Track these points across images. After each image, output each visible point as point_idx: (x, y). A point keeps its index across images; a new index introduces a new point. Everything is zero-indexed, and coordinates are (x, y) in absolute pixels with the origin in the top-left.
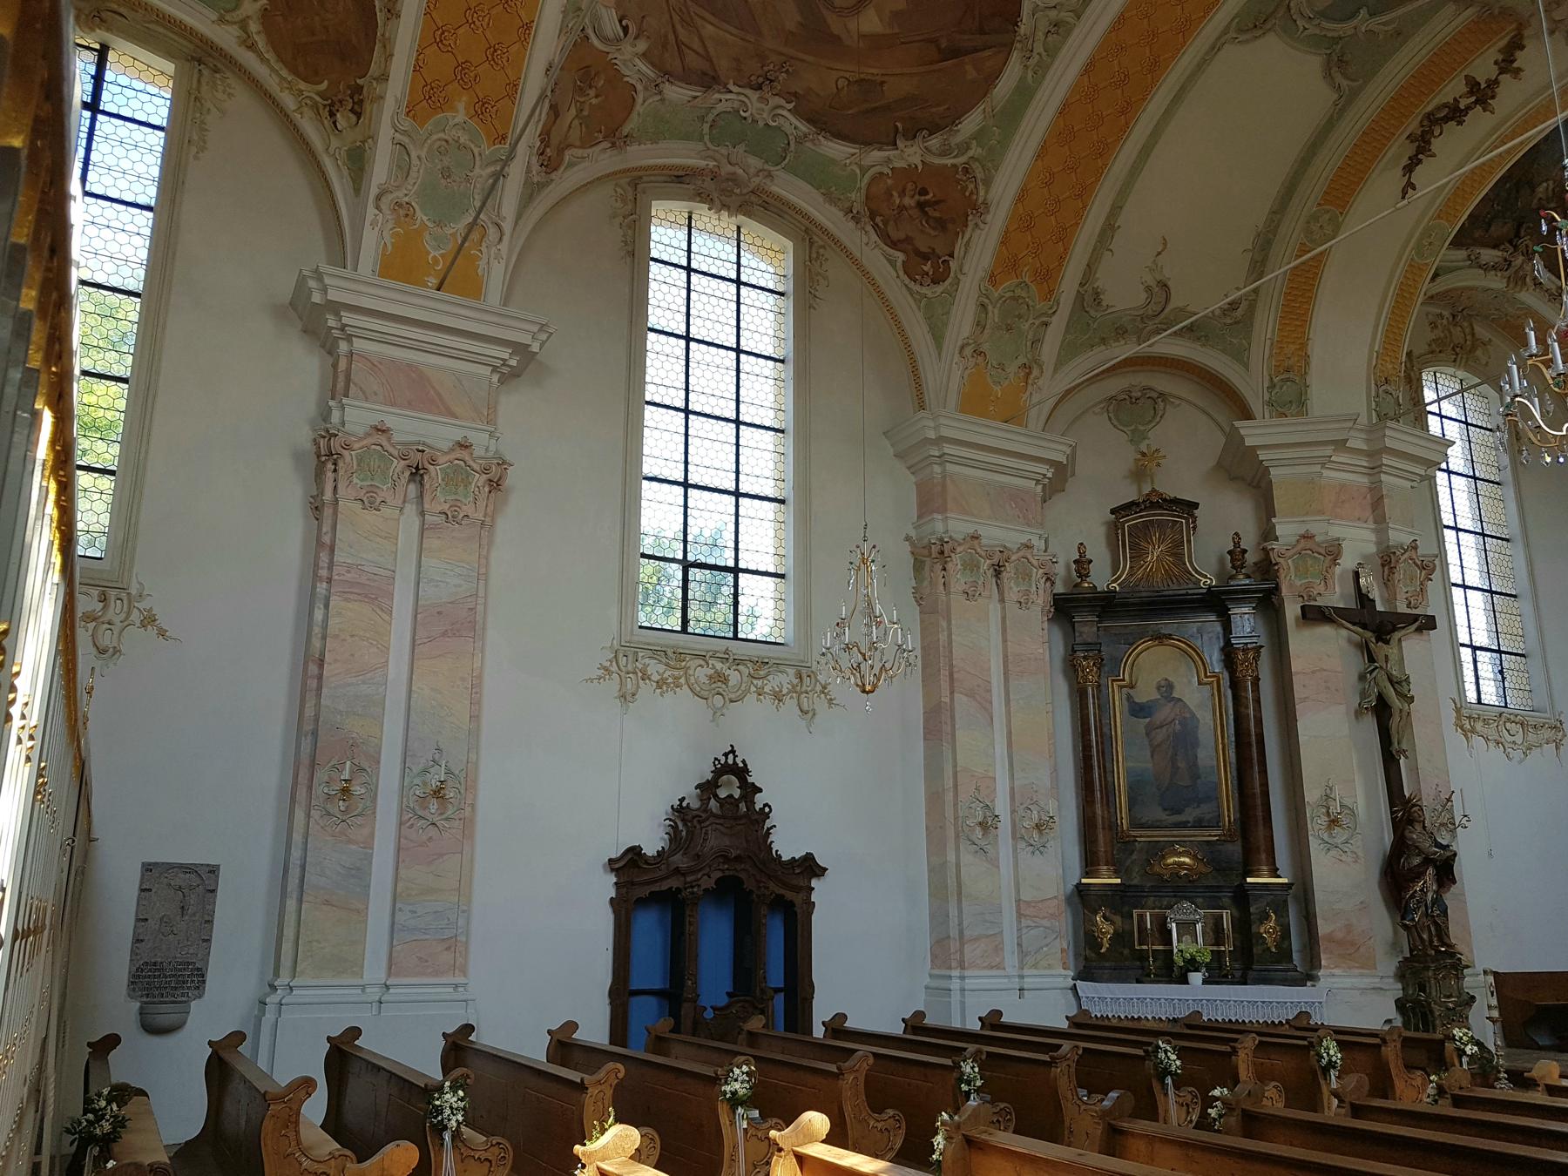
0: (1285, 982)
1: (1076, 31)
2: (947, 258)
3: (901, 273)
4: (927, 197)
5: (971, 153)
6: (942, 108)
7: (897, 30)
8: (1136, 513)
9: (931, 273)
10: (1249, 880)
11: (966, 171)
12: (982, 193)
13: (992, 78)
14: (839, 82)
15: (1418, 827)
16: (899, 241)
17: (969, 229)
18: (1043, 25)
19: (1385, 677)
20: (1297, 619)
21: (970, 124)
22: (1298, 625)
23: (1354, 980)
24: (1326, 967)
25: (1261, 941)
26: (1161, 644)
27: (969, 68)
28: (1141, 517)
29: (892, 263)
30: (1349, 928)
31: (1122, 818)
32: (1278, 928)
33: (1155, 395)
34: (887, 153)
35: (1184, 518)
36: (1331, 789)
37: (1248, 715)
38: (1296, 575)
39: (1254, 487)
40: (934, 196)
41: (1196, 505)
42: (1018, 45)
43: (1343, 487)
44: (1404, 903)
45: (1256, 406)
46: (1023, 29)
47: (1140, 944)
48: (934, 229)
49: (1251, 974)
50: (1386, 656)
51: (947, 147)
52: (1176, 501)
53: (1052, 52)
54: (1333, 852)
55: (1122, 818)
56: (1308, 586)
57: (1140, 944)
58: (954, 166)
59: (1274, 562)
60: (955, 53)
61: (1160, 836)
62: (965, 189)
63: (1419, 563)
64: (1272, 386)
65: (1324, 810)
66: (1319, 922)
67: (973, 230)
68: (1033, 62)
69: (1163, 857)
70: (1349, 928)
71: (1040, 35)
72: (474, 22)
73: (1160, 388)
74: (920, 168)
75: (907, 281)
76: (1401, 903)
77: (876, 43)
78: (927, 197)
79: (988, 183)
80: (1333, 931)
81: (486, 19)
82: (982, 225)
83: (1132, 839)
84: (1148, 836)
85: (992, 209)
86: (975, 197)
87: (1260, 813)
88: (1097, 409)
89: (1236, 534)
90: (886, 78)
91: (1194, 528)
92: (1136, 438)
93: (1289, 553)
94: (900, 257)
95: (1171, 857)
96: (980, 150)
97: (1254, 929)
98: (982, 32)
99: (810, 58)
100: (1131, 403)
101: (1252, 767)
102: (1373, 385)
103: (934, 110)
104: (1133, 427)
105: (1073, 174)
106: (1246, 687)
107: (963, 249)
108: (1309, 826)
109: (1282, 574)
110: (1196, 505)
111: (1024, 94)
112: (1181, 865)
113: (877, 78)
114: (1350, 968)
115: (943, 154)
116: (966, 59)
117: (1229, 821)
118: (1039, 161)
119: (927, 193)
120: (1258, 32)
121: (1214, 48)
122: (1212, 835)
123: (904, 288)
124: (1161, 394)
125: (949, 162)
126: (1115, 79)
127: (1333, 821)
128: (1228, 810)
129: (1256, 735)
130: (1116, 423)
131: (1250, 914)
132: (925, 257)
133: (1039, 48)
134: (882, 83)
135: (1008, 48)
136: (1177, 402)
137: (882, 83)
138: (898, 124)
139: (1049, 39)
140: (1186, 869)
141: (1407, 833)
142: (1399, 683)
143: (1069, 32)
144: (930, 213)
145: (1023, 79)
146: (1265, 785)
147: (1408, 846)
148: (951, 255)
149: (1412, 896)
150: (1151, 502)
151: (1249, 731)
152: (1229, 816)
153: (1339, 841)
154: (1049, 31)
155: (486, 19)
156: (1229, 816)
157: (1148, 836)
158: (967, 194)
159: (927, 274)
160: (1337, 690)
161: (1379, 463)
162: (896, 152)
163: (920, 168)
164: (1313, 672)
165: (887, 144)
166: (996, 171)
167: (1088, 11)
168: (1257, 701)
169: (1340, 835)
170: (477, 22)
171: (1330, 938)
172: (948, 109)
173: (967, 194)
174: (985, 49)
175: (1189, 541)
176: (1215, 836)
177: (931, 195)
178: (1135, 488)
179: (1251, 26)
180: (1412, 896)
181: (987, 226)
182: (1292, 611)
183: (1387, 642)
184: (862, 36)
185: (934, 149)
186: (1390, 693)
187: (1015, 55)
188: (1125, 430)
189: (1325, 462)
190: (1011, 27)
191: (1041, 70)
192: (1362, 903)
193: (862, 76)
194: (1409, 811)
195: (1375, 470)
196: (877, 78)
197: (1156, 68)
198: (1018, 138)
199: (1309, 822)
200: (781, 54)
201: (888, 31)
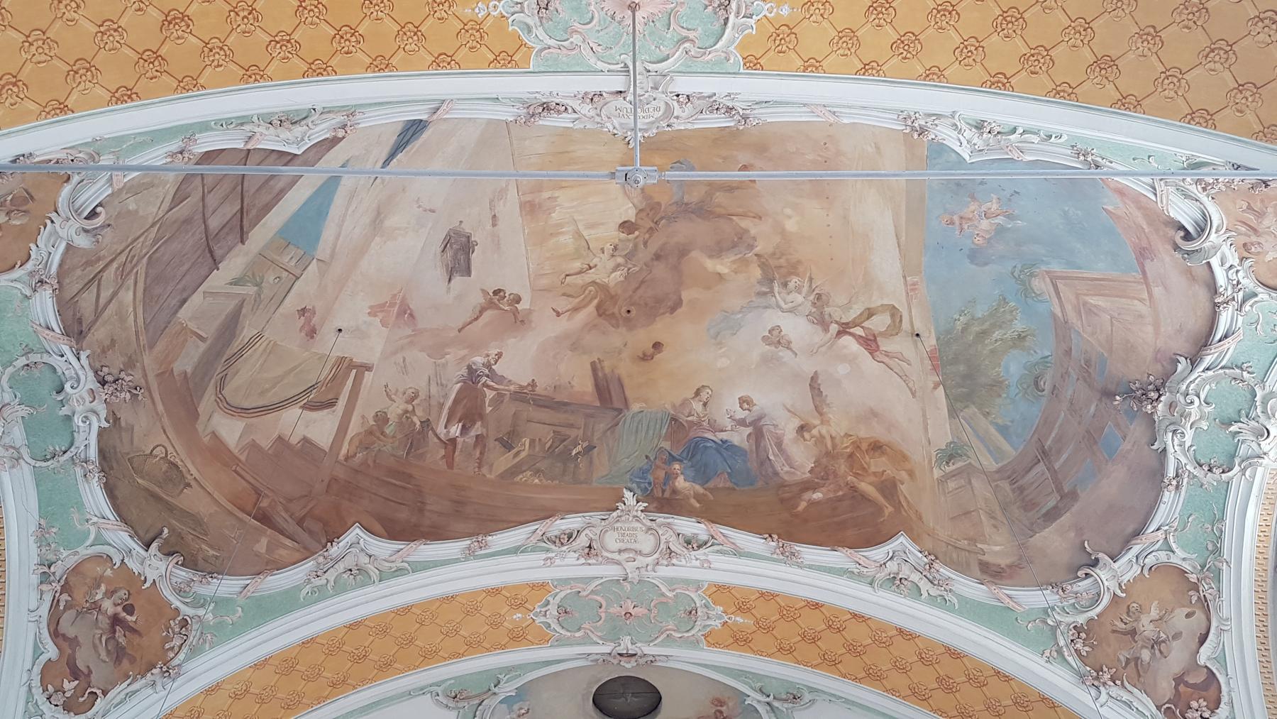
1: (371, 589)
2: (99, 692)
3: (37, 670)
4: (129, 618)
5: (201, 612)
6: (212, 552)
7: (243, 458)
9: (68, 695)
11: (184, 623)
12: (181, 656)
13: (278, 566)
14: (158, 448)
16: (64, 635)
17: (143, 681)
18: (349, 562)
21: (227, 586)
27: (264, 541)
29: (37, 653)
34: (135, 546)
40: (135, 622)
42: (321, 559)
46: (334, 550)
48: (108, 652)
51: (188, 589)
53: (339, 588)
58: (177, 609)
60: (265, 519)
62: (168, 639)
67: (146, 686)
68: (318, 582)
71: (341, 567)
72: (31, 44)
74: (147, 585)
75: (36, 682)
77: (217, 452)
78: (129, 618)
79: (195, 652)
81: (43, 58)
82: (159, 687)
85: (179, 681)
86: (172, 655)
90: (193, 483)
94: (51, 652)
96: (210, 616)
98: (300, 522)
99: (160, 408)
103: (203, 546)
105: (258, 705)
107: (122, 695)
111: (287, 603)
113: (189, 477)
115: (179, 591)
116: (269, 531)
118: (252, 670)
119: (131, 614)
120: (452, 704)
121: (422, 689)
123: (25, 689)
125: (176, 603)
126: (357, 652)
132: (75, 673)
133: (331, 575)
134: (189, 485)
135: (308, 553)
137: (189, 485)
138: (166, 530)
139: (345, 576)
143: (363, 585)
144: (117, 635)
145: (298, 588)
148: (105, 693)
154: (351, 570)
155: (43, 58)
158: (167, 646)
159: (64, 693)
162: (142, 552)
163: (147, 585)
165: (140, 539)
166: (211, 648)
167: (393, 582)
170: (33, 49)
172: (217, 557)
173: (167, 646)
174: (288, 537)
177: (134, 618)
179: (453, 694)
181: (164, 693)
184: (214, 435)
185: (174, 580)
187: (309, 565)
190: (324, 541)
191: (320, 594)
193: (180, 463)
196: (189, 477)
197: (386, 668)
198: (254, 634)
200: (145, 376)
201: (236, 452)
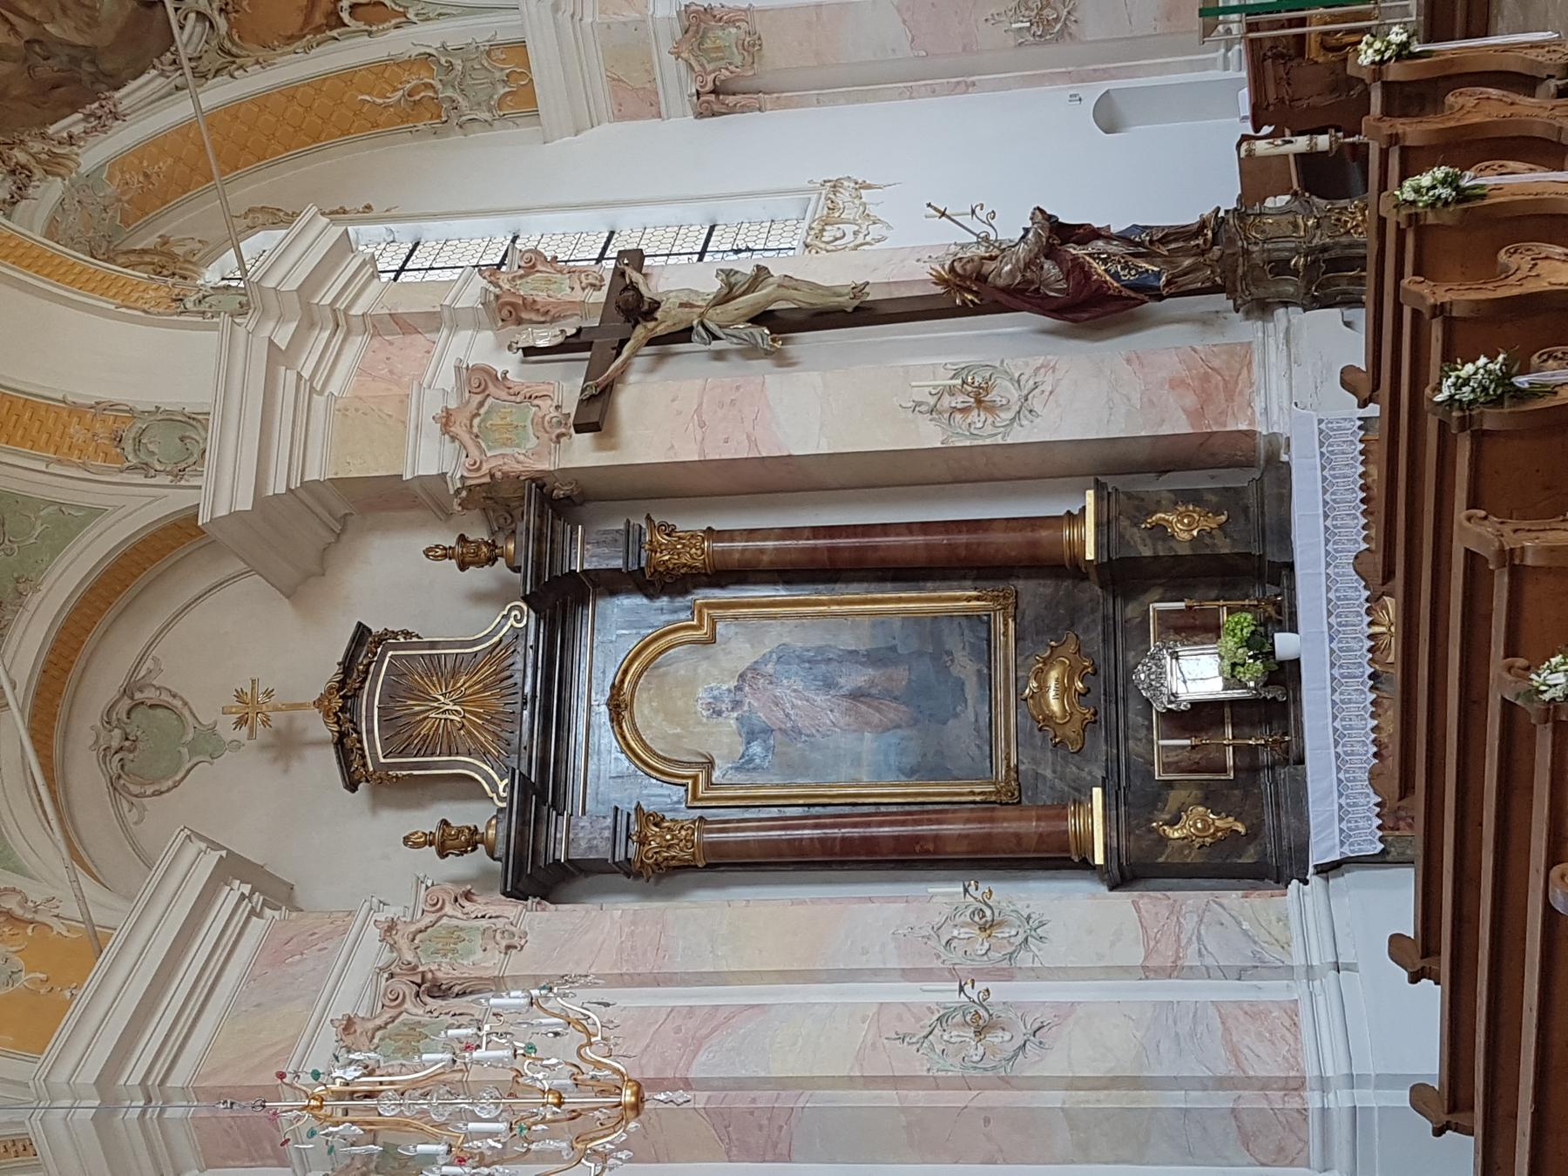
0: (1285, 499)
8: (360, 741)
10: (1090, 556)
15: (989, 266)
19: (719, 309)
20: (600, 448)
22: (612, 448)
23: (1274, 378)
24: (1252, 422)
25: (1208, 540)
26: (629, 706)
28: (370, 731)
30: (1176, 384)
31: (973, 793)
32: (1182, 509)
33: (126, 703)
35: (383, 655)
36: (919, 404)
37: (776, 549)
38: (518, 446)
39: (343, 530)
41: (362, 632)
43: (362, 371)
44: (1125, 292)
45: (174, 501)
47: (1224, 770)
49: (1273, 555)
50: (682, 305)
52: (348, 665)
54: (1036, 403)
55: (973, 793)
56: (539, 423)
57: (1224, 770)
59: (487, 480)
61: (1009, 721)
63: (521, 272)
64: (144, 468)
65: (958, 416)
66: (1166, 430)
69: (1049, 718)
70: (1176, 384)
73: (113, 693)
76: (1129, 298)
80: (1184, 410)
83: (1013, 774)
84: (1008, 745)
87: (963, 538)
88: (132, 817)
89: (427, 553)
91: (407, 634)
92: (209, 745)
93: (474, 452)
95: (1048, 705)
97: (1184, 551)
100: (131, 751)
101: (875, 548)
102: (182, 318)
104: (185, 750)
106: (723, 552)
108: (988, 442)
109: (513, 467)
110: (362, 632)
112: (1063, 691)
114: (1252, 384)
117: (978, 599)
122: (1005, 630)
124: (127, 692)
127: (979, 402)
128: (958, 599)
129: (815, 538)
130: (170, 783)
131: (1156, 558)
136: (149, 664)
140: (1071, 681)
141: (1001, 282)
142: (731, 287)
146: (909, 527)
147: (1025, 281)
149: (1116, 276)
150: (342, 709)
151: (803, 550)
152: (969, 599)
153: (1014, 394)
156: (969, 599)
157: (1008, 745)
160: (738, 388)
161: (328, 313)
164: (702, 425)
168: (751, 534)
169: (1004, 392)
171: (1196, 414)
175: (433, 645)
176: (1006, 625)
178: (310, 753)
180: (1116, 276)
182: (582, 453)
183: (656, 305)
186: (746, 303)
188: (188, 766)
189: (308, 389)
192: (1128, 361)
194: (962, 277)
195: (340, 321)
199: (980, 442)
